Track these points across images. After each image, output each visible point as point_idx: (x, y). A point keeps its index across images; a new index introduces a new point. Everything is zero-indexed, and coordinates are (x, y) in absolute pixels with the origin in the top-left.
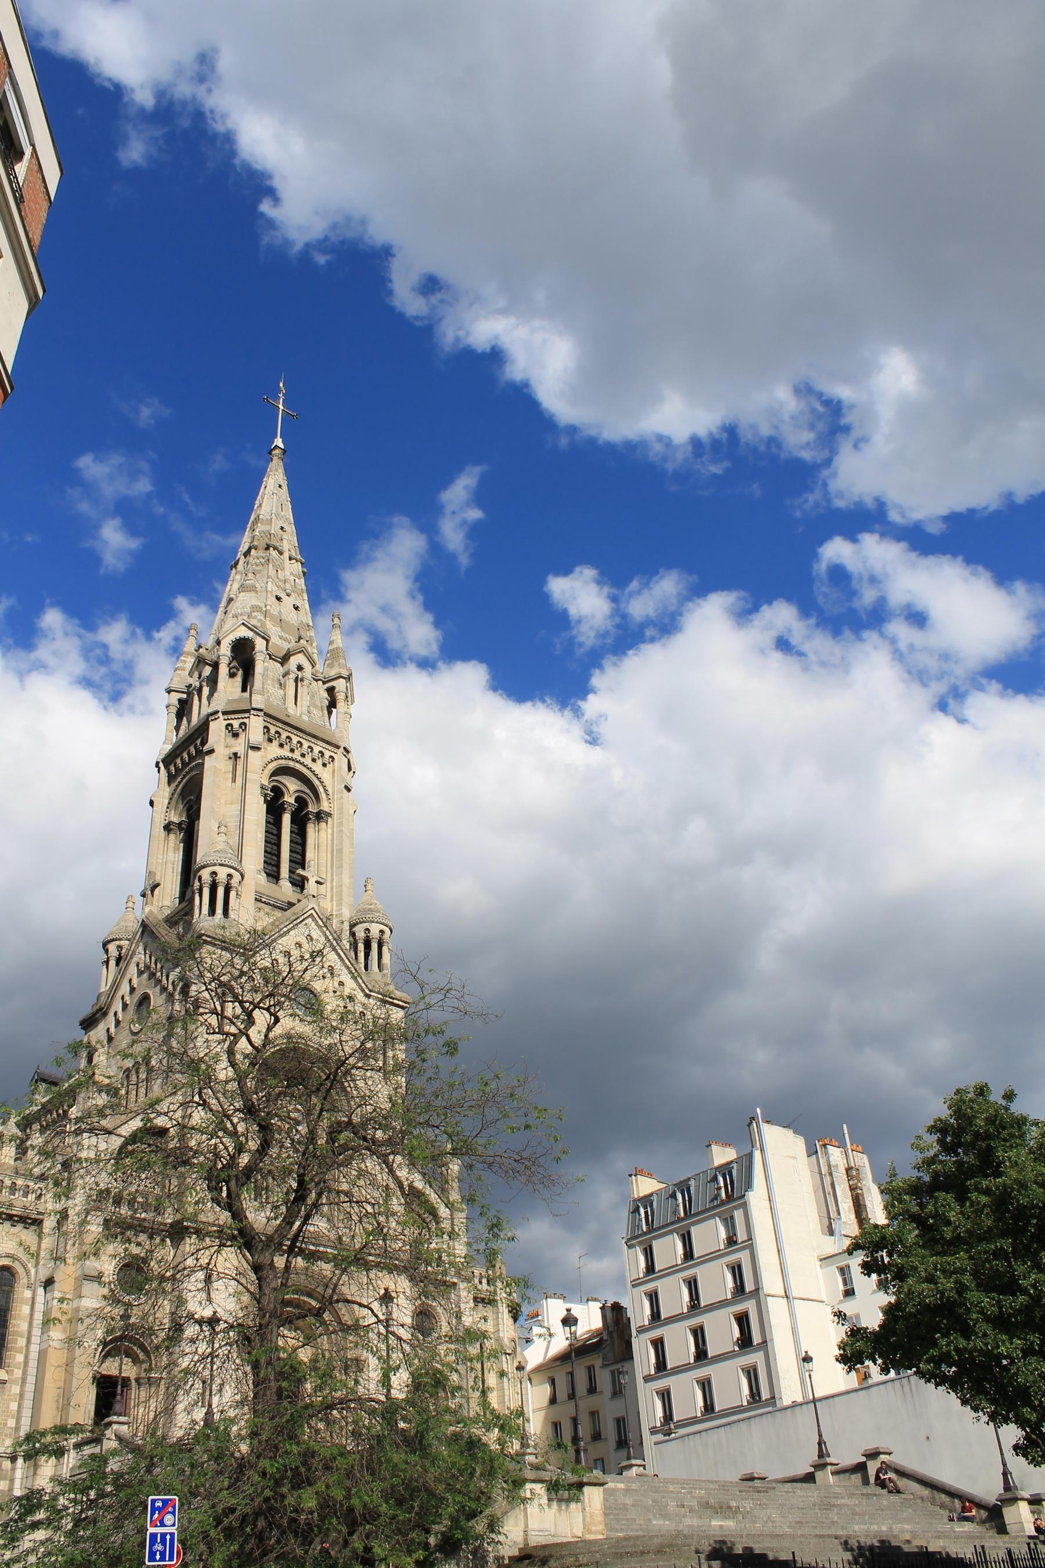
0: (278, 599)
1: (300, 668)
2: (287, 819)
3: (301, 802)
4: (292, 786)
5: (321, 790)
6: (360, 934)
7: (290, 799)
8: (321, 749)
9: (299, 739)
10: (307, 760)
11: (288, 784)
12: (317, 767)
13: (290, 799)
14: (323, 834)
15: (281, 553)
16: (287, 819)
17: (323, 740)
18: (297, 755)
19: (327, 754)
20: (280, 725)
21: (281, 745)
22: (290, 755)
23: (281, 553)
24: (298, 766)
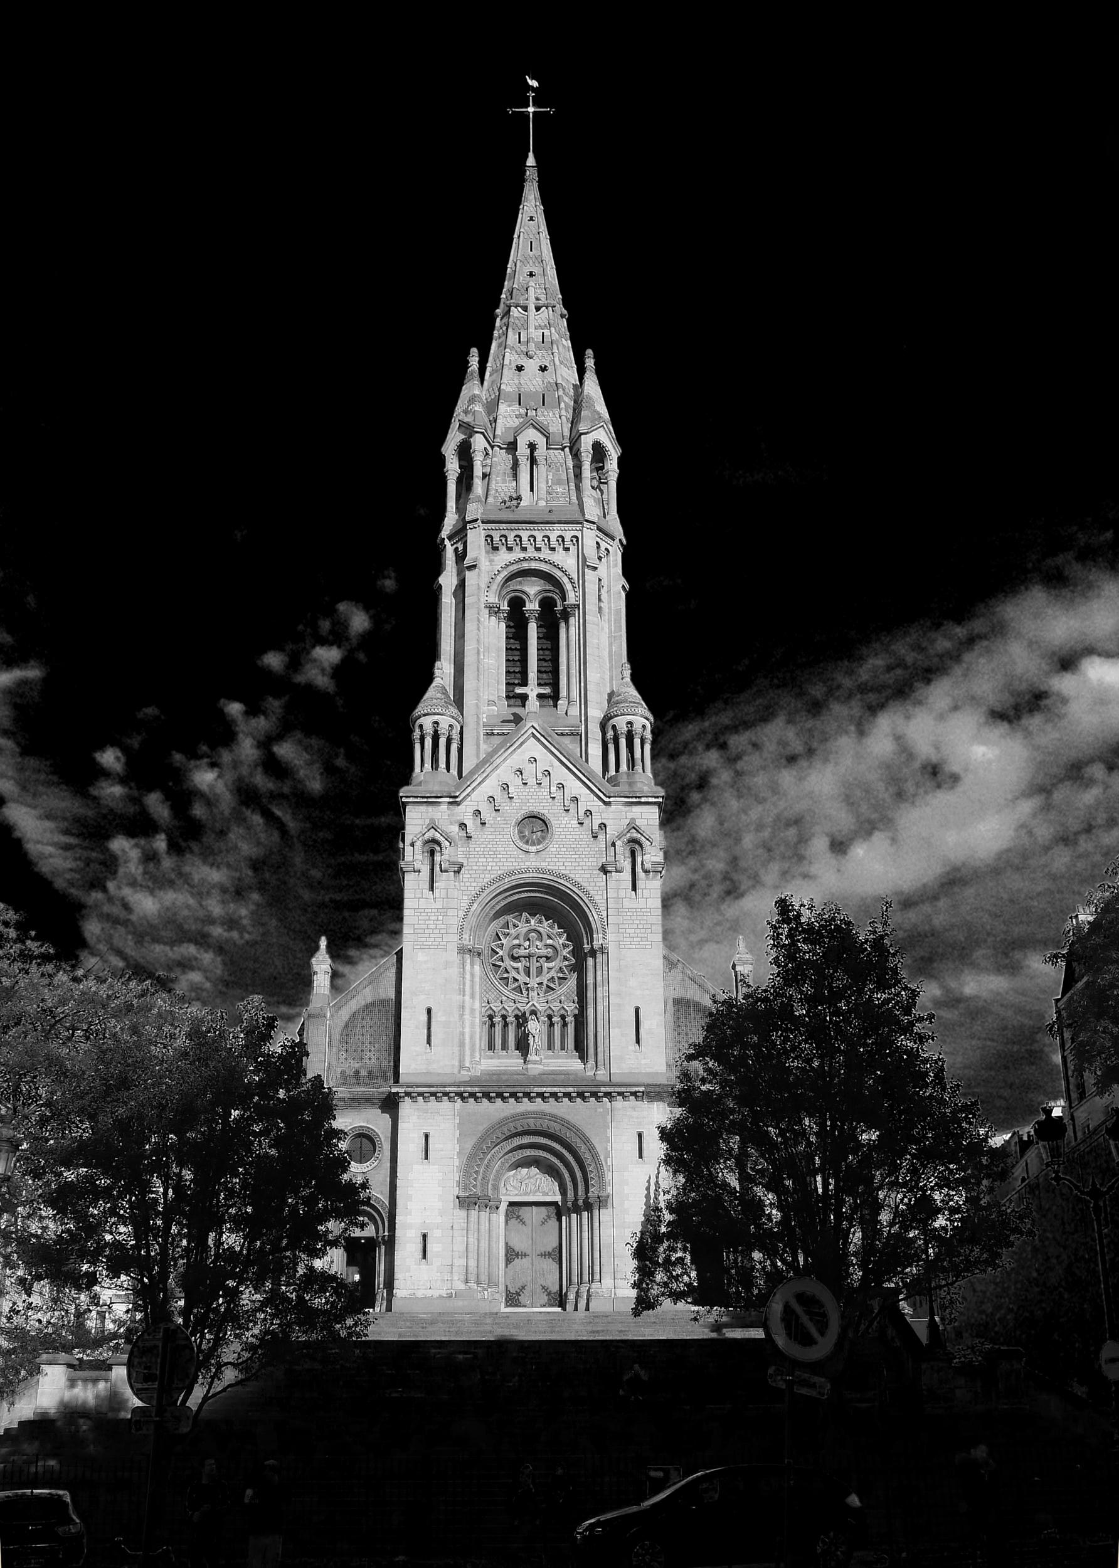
0: (520, 369)
1: (532, 447)
3: (547, 604)
4: (533, 589)
5: (565, 580)
6: (610, 734)
7: (532, 606)
8: (559, 533)
9: (529, 533)
10: (545, 554)
11: (519, 587)
12: (559, 557)
13: (532, 606)
14: (573, 631)
15: (525, 309)
17: (560, 522)
18: (531, 553)
19: (568, 536)
20: (504, 526)
21: (510, 549)
22: (522, 555)
23: (525, 309)
24: (534, 565)
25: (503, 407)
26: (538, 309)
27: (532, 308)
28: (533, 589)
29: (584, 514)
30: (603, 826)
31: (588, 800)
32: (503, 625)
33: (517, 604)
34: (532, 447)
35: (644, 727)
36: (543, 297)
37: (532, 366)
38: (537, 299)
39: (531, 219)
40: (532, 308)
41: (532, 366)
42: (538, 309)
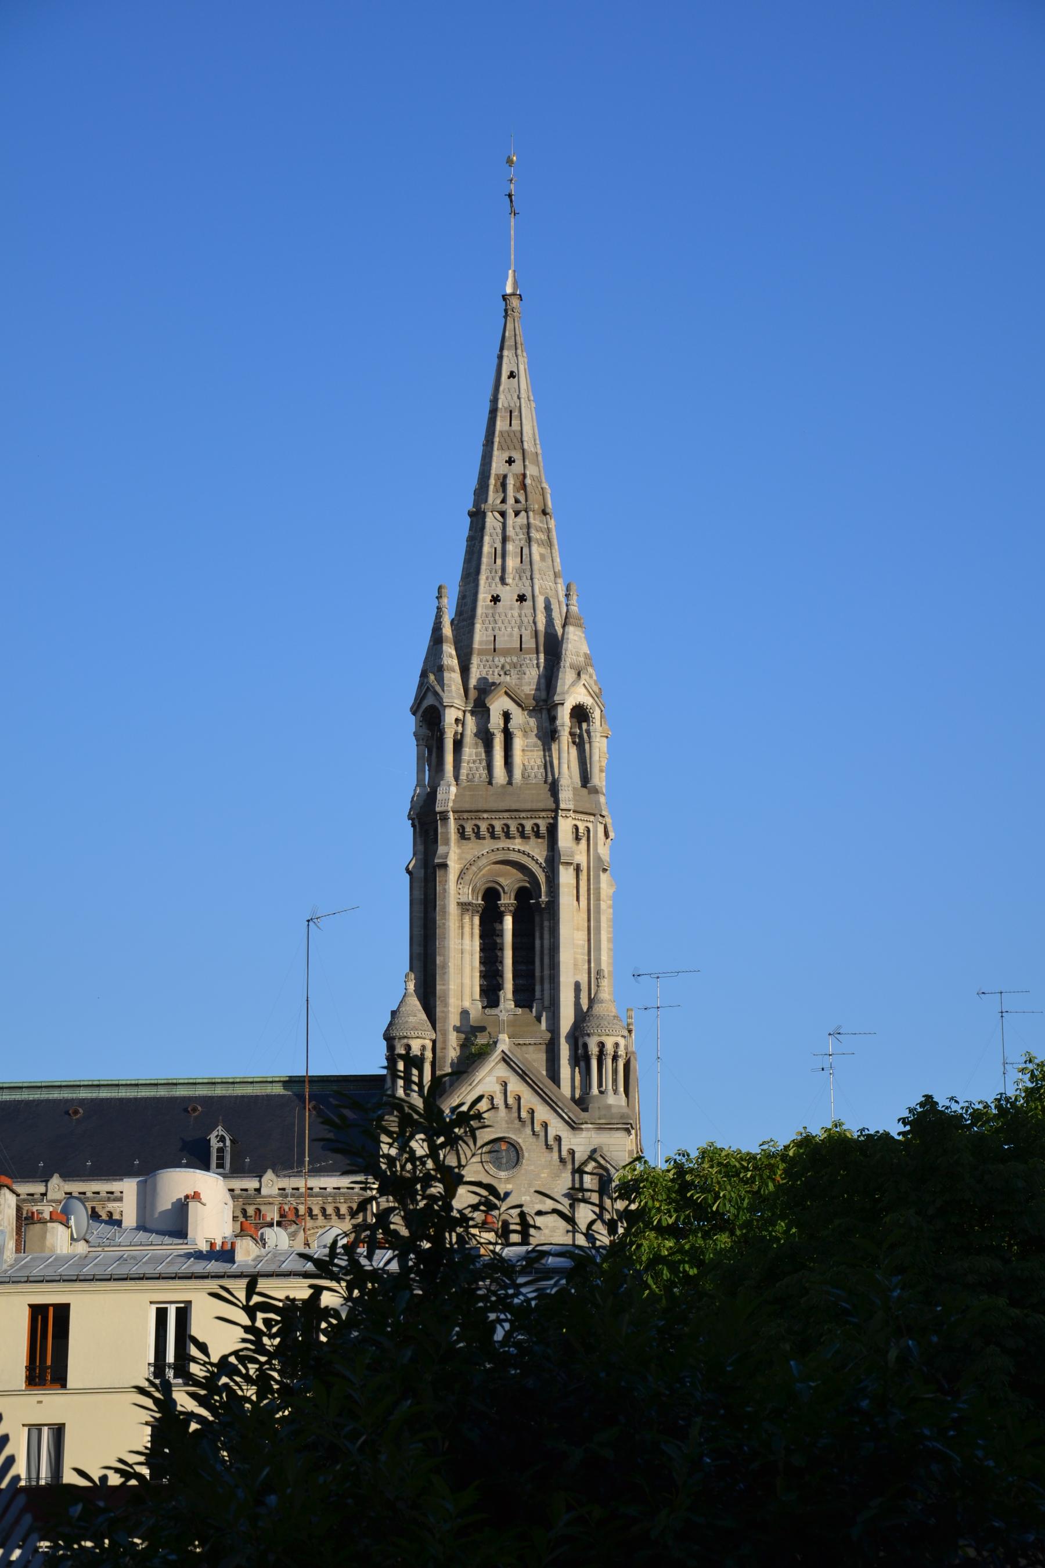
1: (507, 716)
2: (508, 922)
3: (523, 895)
7: (507, 900)
13: (507, 900)
16: (508, 922)
23: (503, 514)
25: (475, 660)
26: (517, 514)
27: (510, 513)
28: (510, 882)
29: (557, 801)
30: (572, 1153)
31: (557, 1127)
32: (477, 920)
33: (491, 895)
34: (507, 716)
35: (617, 1045)
36: (522, 499)
37: (508, 595)
38: (517, 501)
39: (512, 375)
40: (510, 513)
41: (508, 595)
42: (517, 514)
